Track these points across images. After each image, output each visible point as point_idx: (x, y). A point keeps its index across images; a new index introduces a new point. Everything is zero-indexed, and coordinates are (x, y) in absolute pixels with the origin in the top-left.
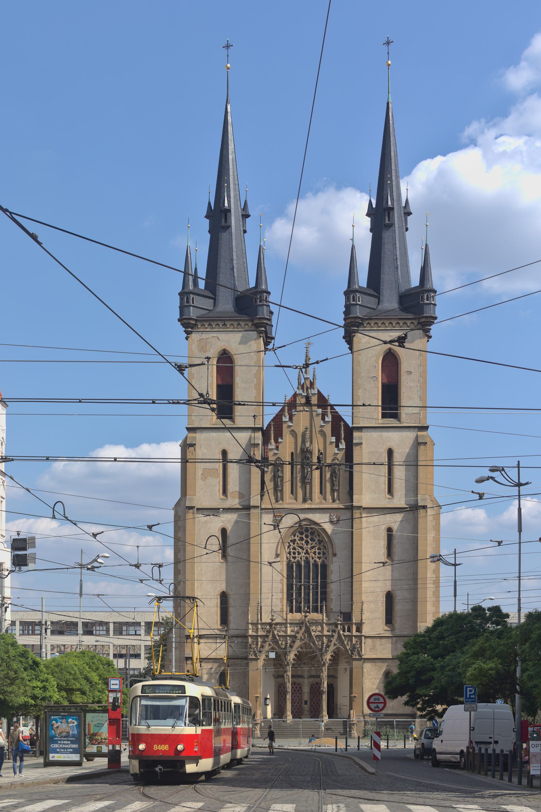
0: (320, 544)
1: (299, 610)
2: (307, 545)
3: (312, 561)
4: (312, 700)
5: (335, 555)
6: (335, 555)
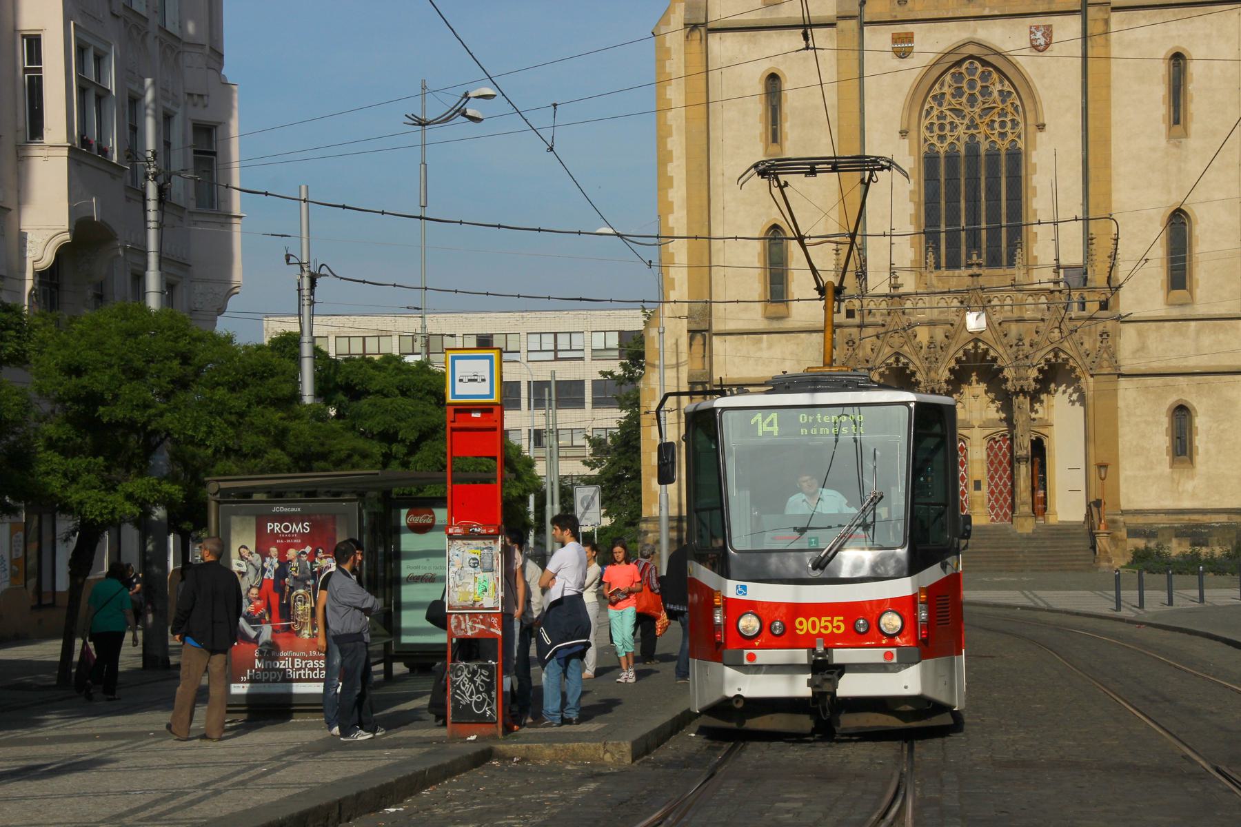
0: (1003, 102)
1: (953, 264)
2: (972, 106)
3: (984, 147)
4: (992, 478)
5: (1041, 127)
6: (1041, 127)
